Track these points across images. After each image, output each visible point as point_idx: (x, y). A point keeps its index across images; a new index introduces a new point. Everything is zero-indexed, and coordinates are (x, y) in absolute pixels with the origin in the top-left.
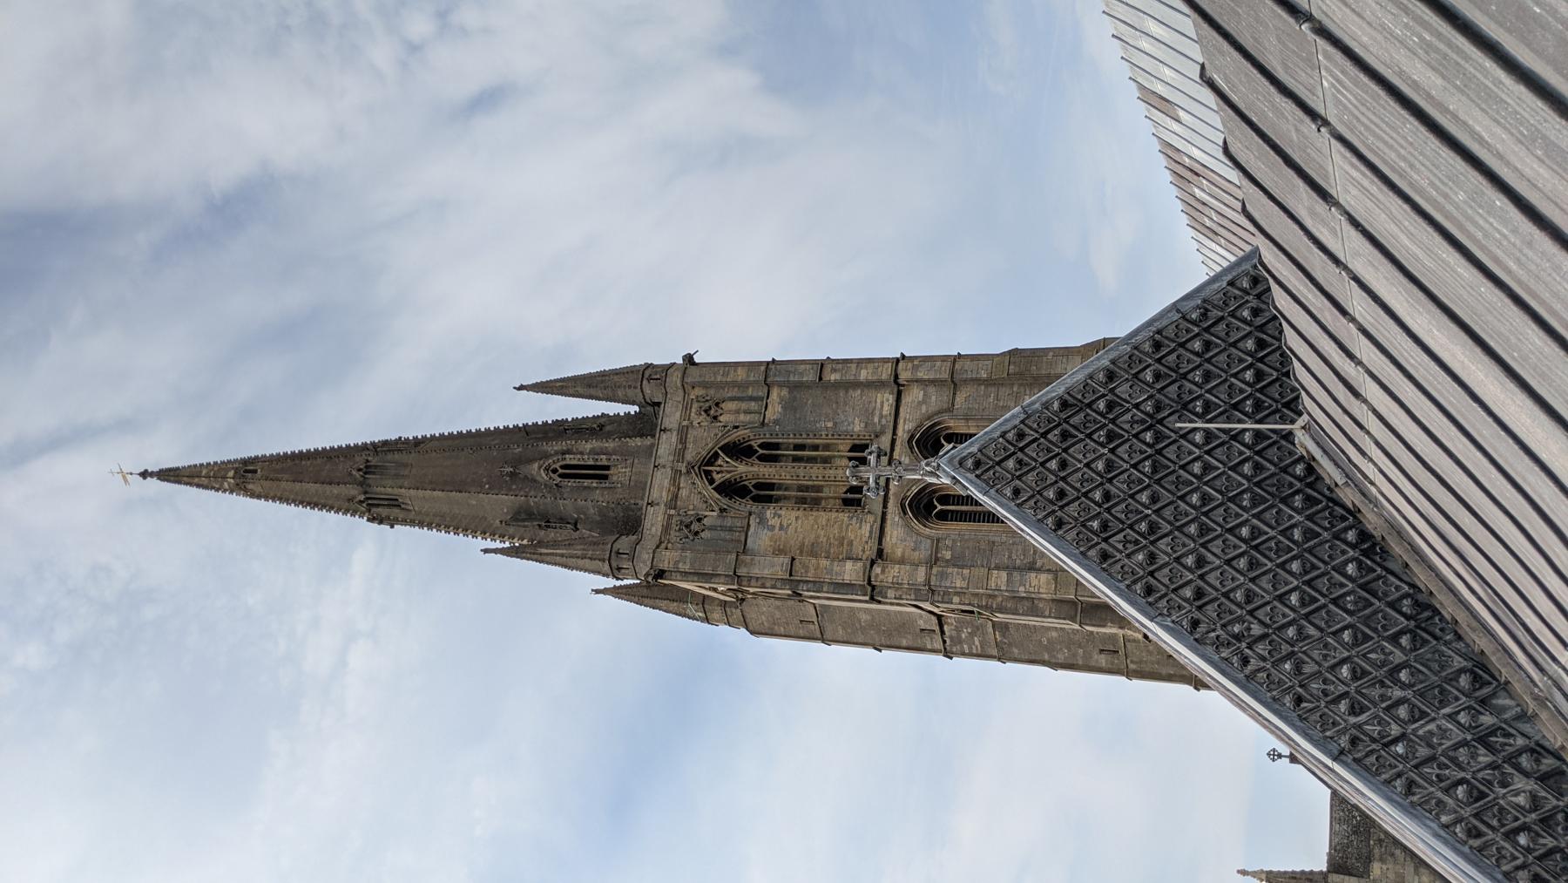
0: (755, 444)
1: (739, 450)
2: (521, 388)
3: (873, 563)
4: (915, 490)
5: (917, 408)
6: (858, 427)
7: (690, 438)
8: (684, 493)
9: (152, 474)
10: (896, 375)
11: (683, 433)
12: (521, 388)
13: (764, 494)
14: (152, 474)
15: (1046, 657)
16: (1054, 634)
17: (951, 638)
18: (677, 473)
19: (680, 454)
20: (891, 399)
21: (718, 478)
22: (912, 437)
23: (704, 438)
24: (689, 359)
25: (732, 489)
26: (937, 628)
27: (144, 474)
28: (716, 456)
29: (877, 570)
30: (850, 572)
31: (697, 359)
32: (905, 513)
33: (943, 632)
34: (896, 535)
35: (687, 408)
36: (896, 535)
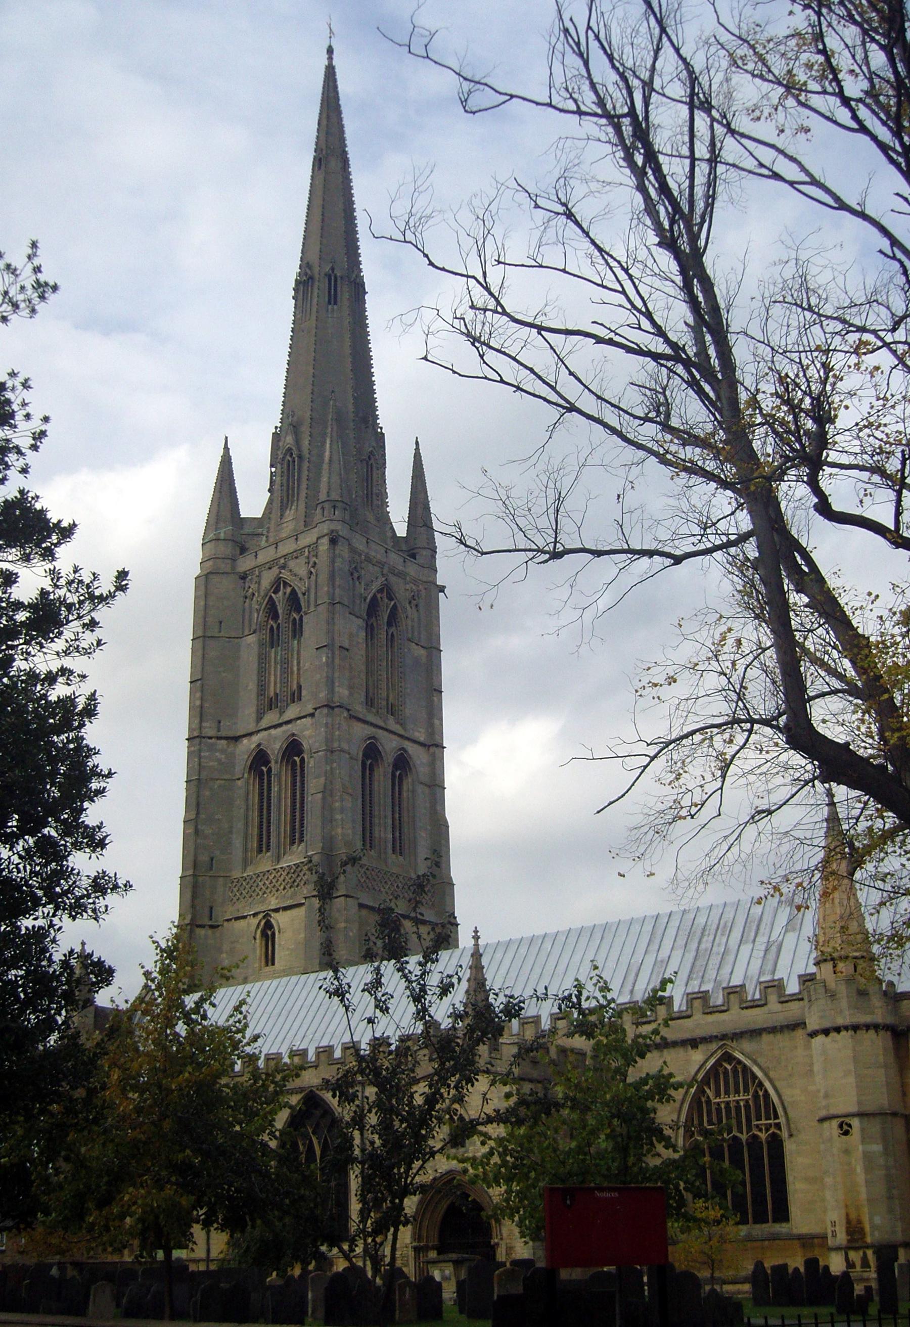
0: (393, 629)
1: (393, 619)
2: (417, 443)
3: (348, 710)
4: (380, 748)
5: (418, 755)
6: (408, 712)
7: (400, 581)
8: (371, 567)
9: (330, 59)
10: (435, 746)
11: (401, 575)
12: (417, 443)
13: (370, 630)
14: (330, 59)
15: (203, 816)
16: (226, 826)
17: (212, 745)
18: (381, 565)
19: (392, 571)
20: (422, 739)
21: (379, 596)
22: (406, 751)
23: (402, 591)
24: (442, 589)
25: (373, 608)
26: (223, 733)
27: (330, 51)
28: (391, 599)
29: (345, 714)
30: (342, 692)
31: (441, 594)
32: (369, 738)
33: (219, 738)
34: (360, 731)
35: (415, 581)
36: (360, 731)
